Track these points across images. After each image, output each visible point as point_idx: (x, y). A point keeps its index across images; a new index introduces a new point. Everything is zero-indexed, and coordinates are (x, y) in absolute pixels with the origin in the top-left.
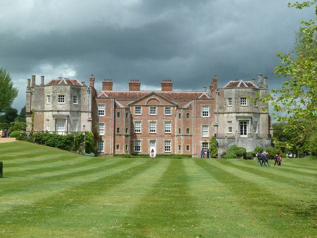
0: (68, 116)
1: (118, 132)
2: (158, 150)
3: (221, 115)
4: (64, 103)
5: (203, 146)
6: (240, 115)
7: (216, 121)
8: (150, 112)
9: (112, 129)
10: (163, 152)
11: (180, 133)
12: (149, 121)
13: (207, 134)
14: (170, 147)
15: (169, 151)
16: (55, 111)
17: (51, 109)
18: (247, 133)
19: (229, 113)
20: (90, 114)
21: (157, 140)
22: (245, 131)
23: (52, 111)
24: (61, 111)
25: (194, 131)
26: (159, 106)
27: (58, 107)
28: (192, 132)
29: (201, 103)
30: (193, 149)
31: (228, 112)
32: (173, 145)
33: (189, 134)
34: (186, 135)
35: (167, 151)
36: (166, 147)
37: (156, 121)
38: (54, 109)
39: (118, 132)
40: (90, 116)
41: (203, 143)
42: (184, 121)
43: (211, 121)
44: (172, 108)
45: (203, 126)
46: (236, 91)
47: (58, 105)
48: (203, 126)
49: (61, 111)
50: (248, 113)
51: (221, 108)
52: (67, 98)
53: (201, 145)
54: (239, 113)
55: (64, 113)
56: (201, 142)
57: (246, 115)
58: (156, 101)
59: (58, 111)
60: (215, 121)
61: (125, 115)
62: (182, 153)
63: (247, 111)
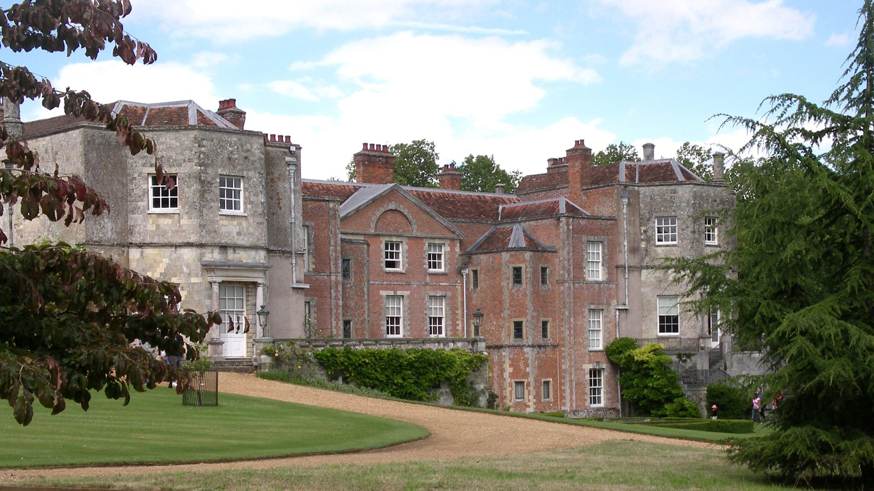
11: (545, 335)
12: (384, 293)
16: (213, 246)
17: (193, 239)
23: (201, 246)
24: (236, 247)
26: (409, 238)
27: (223, 230)
33: (550, 340)
37: (406, 293)
43: (610, 297)
44: (445, 249)
45: (590, 310)
47: (225, 222)
48: (590, 310)
49: (236, 247)
51: (634, 250)
53: (588, 377)
55: (245, 257)
56: (588, 367)
58: (399, 218)
59: (224, 248)
60: (621, 297)
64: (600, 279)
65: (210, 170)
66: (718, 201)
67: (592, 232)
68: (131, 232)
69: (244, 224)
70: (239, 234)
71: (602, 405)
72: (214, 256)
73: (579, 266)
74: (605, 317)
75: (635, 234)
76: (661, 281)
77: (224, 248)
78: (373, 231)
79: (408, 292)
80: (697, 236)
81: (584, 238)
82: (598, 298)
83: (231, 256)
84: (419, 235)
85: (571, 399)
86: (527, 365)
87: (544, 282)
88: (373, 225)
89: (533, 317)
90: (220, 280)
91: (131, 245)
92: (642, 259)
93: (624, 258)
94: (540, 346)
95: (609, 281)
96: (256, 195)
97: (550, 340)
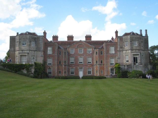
0: (28, 53)
1: (60, 63)
2: (84, 73)
3: (121, 52)
4: (26, 46)
5: (111, 71)
6: (133, 51)
7: (118, 56)
8: (79, 52)
9: (56, 62)
10: (87, 74)
12: (78, 57)
14: (91, 72)
15: (90, 74)
17: (18, 50)
18: (138, 62)
19: (126, 50)
20: (42, 52)
21: (83, 68)
22: (137, 61)
23: (19, 50)
24: (24, 50)
25: (105, 62)
28: (104, 62)
29: (109, 45)
30: (105, 72)
31: (126, 49)
32: (93, 71)
34: (101, 64)
35: (89, 74)
36: (88, 72)
38: (20, 50)
39: (60, 63)
40: (42, 54)
41: (111, 69)
42: (99, 56)
46: (131, 37)
49: (24, 50)
50: (138, 50)
52: (27, 42)
53: (110, 70)
54: (133, 50)
55: (25, 52)
56: (110, 68)
57: (137, 51)
59: (22, 51)
61: (64, 53)
62: (98, 75)
63: (138, 49)
64: (114, 53)
65: (21, 40)
66: (137, 38)
67: (111, 45)
68: (15, 50)
69: (26, 47)
70: (25, 48)
71: (114, 75)
72: (21, 52)
73: (108, 51)
74: (114, 59)
75: (122, 45)
76: (126, 53)
77: (22, 51)
78: (77, 48)
79: (83, 57)
80: (131, 44)
81: (109, 46)
82: (113, 56)
83: (23, 52)
84: (86, 48)
85: (106, 74)
86: (98, 68)
87: (102, 54)
88: (77, 47)
89: (99, 60)
90: (20, 55)
91: (16, 51)
92: (123, 49)
93: (118, 49)
94: (100, 65)
95: (115, 53)
96: (28, 43)
97: (103, 64)
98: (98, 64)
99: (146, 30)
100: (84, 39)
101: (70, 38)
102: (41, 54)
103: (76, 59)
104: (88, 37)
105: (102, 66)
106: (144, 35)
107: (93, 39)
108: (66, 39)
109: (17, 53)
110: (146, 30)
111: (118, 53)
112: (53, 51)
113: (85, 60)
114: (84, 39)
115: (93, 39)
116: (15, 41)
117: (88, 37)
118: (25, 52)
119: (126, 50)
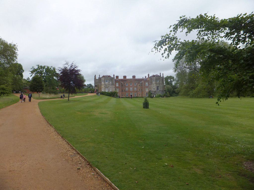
6: (157, 85)
13: (147, 90)
19: (153, 84)
32: (137, 94)
55: (107, 86)
57: (159, 85)
82: (147, 87)
83: (106, 86)
98: (140, 91)
99: (163, 74)
100: (132, 78)
101: (125, 77)
102: (114, 86)
103: (129, 89)
104: (134, 77)
105: (142, 92)
106: (162, 76)
107: (136, 78)
108: (122, 78)
109: (102, 86)
110: (163, 74)
111: (150, 85)
112: (119, 85)
113: (133, 89)
114: (132, 78)
115: (136, 78)
116: (101, 80)
117: (134, 77)
118: (107, 86)
119: (153, 84)
